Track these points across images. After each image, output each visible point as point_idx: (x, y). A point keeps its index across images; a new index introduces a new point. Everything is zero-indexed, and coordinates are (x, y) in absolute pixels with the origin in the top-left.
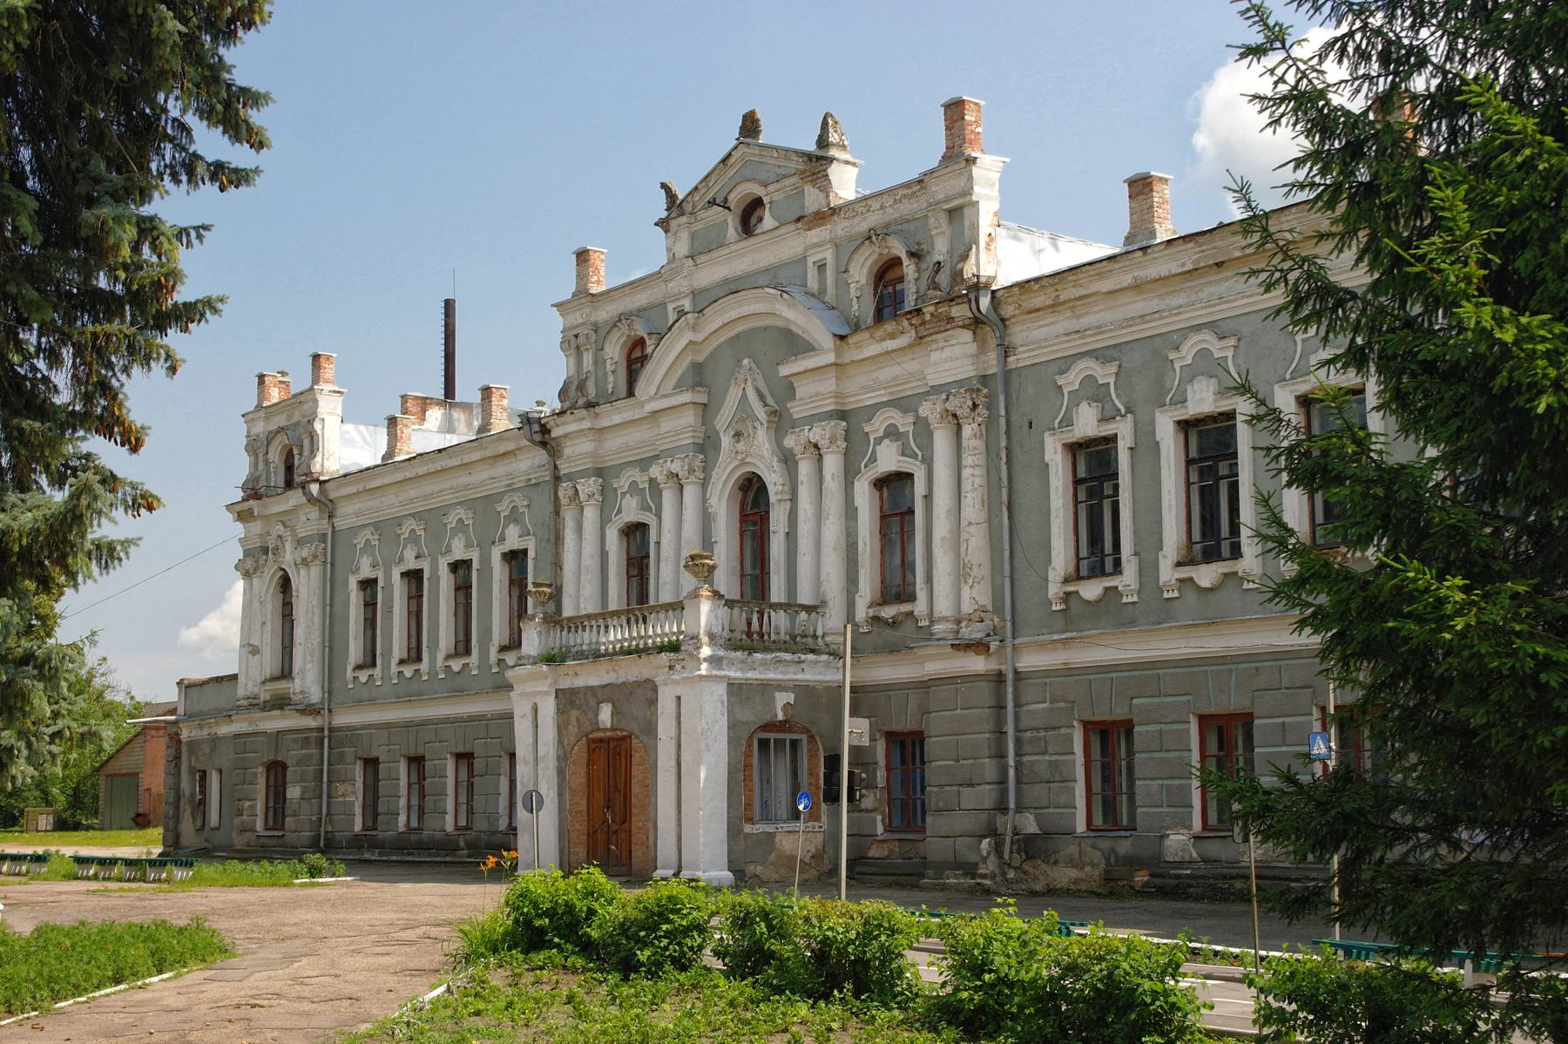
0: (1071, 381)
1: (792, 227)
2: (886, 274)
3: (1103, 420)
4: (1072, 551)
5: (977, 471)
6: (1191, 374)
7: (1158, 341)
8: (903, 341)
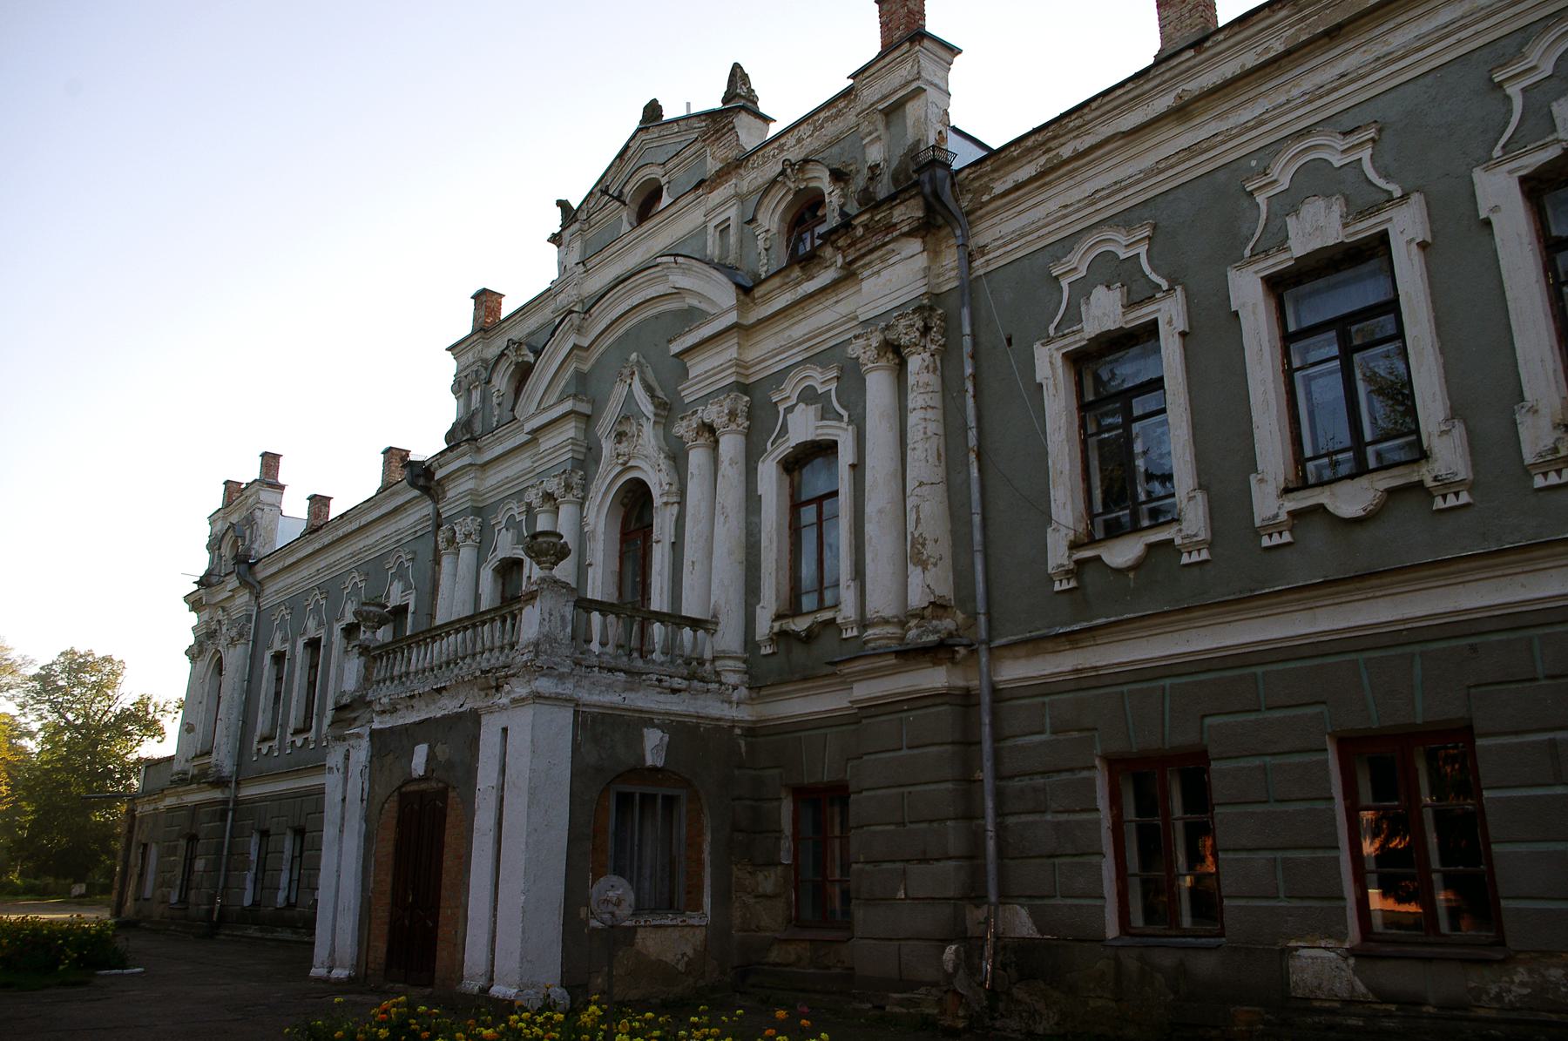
0: (1078, 262)
3: (1131, 305)
4: (1081, 506)
5: (930, 414)
6: (1290, 203)
7: (1221, 177)
8: (825, 277)
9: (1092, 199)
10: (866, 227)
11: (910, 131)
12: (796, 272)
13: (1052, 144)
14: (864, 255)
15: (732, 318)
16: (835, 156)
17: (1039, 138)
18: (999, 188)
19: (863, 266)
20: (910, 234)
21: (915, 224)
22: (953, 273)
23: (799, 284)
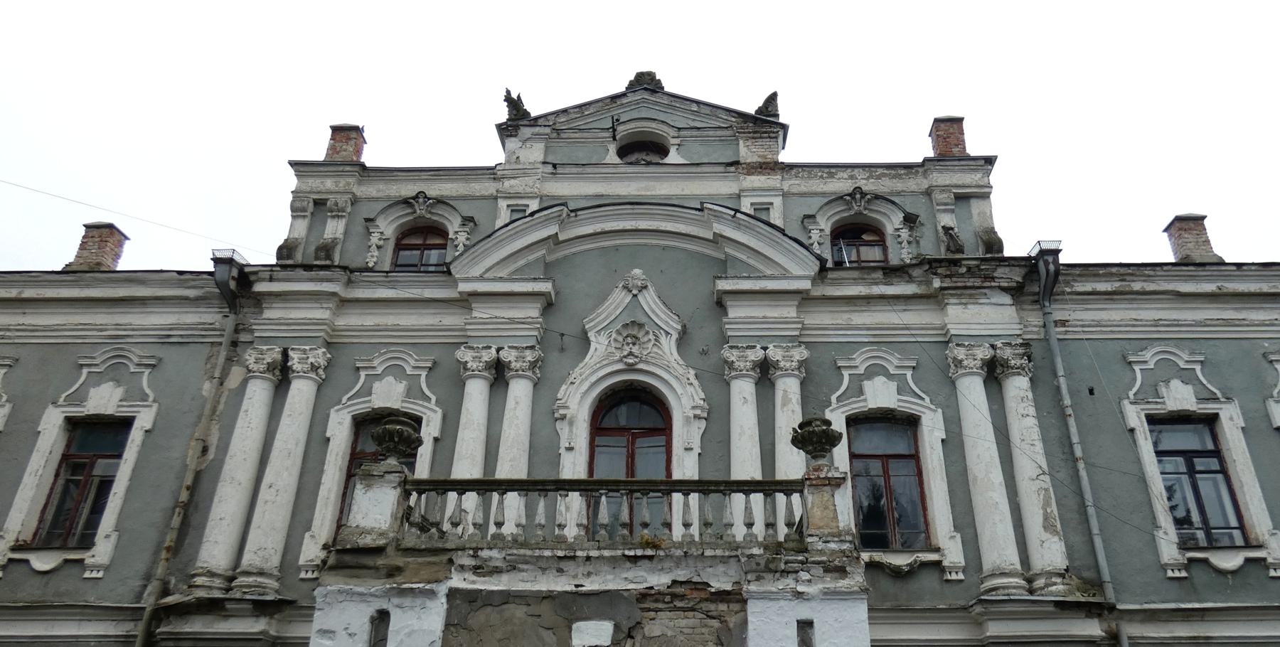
1: (721, 169)
2: (852, 231)
8: (909, 289)
9: (1156, 323)
10: (969, 269)
12: (879, 275)
13: (1128, 278)
15: (805, 285)
16: (917, 206)
17: (1122, 270)
18: (1080, 287)
23: (876, 284)
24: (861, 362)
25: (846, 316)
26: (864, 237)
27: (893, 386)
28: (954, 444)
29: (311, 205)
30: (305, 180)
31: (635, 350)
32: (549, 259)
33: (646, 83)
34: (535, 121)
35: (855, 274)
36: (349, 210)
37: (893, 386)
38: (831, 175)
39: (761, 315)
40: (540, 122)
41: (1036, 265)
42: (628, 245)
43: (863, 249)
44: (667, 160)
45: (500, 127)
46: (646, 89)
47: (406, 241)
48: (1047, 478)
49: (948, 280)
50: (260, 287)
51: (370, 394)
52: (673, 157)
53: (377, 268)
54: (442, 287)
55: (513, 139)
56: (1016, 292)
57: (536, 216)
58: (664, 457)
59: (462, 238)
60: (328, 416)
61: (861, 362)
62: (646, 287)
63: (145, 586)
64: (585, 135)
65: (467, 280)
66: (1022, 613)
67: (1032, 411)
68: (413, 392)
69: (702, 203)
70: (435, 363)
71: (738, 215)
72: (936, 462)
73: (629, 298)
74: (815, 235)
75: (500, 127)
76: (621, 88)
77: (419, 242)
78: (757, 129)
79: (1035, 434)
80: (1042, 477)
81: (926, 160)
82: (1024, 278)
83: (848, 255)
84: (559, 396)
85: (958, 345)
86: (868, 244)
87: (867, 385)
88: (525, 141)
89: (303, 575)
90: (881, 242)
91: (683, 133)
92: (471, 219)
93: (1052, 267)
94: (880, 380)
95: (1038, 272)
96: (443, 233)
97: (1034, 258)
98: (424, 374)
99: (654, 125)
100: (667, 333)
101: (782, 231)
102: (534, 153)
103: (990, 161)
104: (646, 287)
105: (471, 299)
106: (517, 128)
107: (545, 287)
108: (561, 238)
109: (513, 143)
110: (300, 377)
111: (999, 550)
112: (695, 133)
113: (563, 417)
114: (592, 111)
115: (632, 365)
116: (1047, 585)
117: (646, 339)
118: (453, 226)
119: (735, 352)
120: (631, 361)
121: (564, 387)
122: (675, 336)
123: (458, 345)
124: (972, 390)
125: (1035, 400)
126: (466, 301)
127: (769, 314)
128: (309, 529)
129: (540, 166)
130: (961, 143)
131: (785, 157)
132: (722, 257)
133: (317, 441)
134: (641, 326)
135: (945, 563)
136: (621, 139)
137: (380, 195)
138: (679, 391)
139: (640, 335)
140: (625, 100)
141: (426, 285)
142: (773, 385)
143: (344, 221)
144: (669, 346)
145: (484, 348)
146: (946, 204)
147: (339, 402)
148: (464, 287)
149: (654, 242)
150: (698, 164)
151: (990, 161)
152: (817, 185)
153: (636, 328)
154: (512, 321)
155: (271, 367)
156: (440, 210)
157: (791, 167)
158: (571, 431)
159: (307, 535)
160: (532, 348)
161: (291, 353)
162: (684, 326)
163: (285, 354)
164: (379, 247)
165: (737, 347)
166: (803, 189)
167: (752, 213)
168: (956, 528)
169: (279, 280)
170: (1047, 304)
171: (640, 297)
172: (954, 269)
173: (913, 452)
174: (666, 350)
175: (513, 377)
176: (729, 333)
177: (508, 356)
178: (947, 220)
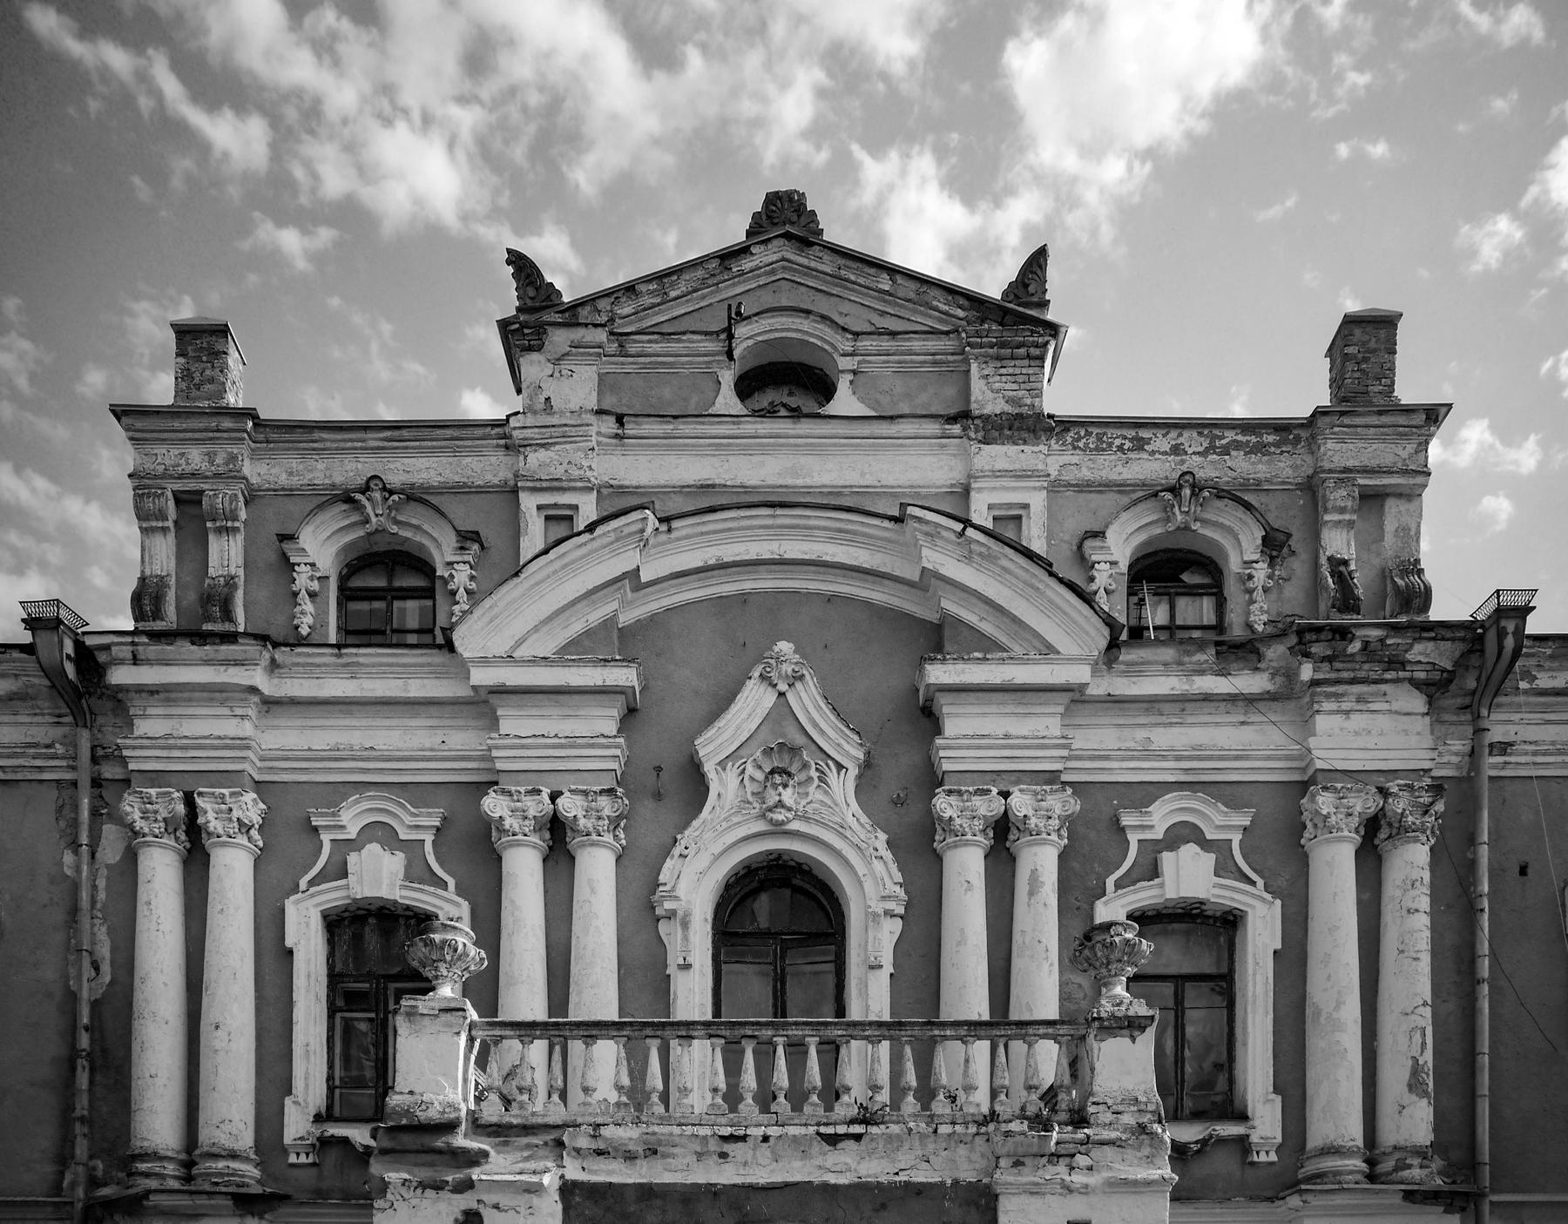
1: (932, 428)
11: (1389, 539)
12: (1207, 656)
14: (1338, 682)
19: (1329, 696)
20: (1416, 684)
21: (1436, 676)
22: (1455, 759)
23: (1201, 673)
24: (1161, 816)
25: (1141, 734)
26: (1186, 577)
27: (1209, 860)
28: (1293, 961)
29: (171, 503)
30: (148, 448)
31: (788, 796)
32: (625, 619)
33: (785, 217)
34: (572, 314)
35: (1168, 653)
36: (243, 515)
37: (1209, 860)
38: (1140, 444)
39: (1000, 732)
40: (584, 314)
41: (1481, 638)
42: (765, 593)
43: (1182, 602)
44: (834, 408)
45: (504, 325)
46: (788, 236)
47: (357, 582)
48: (1429, 1009)
49: (1326, 666)
50: (120, 676)
51: (345, 875)
52: (845, 401)
53: (316, 639)
54: (438, 676)
55: (535, 356)
56: (1434, 688)
57: (599, 531)
58: (831, 980)
59: (462, 577)
60: (283, 911)
61: (1161, 816)
62: (802, 678)
63: (62, 1173)
64: (674, 347)
65: (485, 661)
66: (1355, 1206)
67: (1424, 903)
68: (418, 873)
69: (903, 506)
70: (445, 818)
71: (970, 532)
72: (1260, 989)
73: (770, 698)
74: (1102, 576)
75: (504, 325)
76: (736, 233)
77: (381, 583)
78: (1008, 336)
79: (1422, 940)
80: (1421, 1010)
81: (1319, 413)
82: (1456, 664)
83: (1155, 614)
84: (662, 878)
85: (1325, 788)
86: (1193, 592)
87: (1167, 858)
88: (557, 361)
89: (293, 1159)
90: (1216, 589)
91: (866, 344)
92: (475, 536)
93: (1509, 642)
94: (1189, 850)
95: (1482, 651)
96: (424, 567)
97: (1482, 624)
98: (429, 838)
99: (805, 324)
100: (840, 767)
101: (1046, 565)
102: (577, 389)
103: (1433, 415)
104: (802, 678)
105: (494, 699)
106: (540, 330)
107: (625, 676)
108: (645, 577)
109: (534, 367)
110: (224, 844)
111: (1337, 1115)
112: (886, 344)
113: (671, 915)
114: (683, 287)
115: (782, 823)
116: (1396, 1169)
117: (802, 777)
118: (442, 549)
119: (953, 799)
120: (779, 816)
121: (669, 863)
122: (853, 771)
123: (483, 788)
124: (1335, 867)
125: (1432, 885)
126: (484, 705)
127: (1013, 732)
128: (289, 1092)
129: (591, 418)
130: (1387, 374)
131: (1058, 399)
132: (934, 617)
133: (274, 957)
134: (794, 751)
135: (1254, 1139)
136: (743, 357)
137: (295, 481)
138: (861, 869)
139: (793, 770)
140: (747, 264)
141: (406, 672)
142: (1013, 859)
143: (240, 537)
144: (843, 787)
145: (529, 792)
146: (1342, 510)
147: (295, 889)
148: (482, 677)
149: (813, 586)
150: (892, 418)
151: (1433, 415)
152: (1109, 467)
153: (786, 757)
154: (572, 741)
155: (170, 825)
156: (414, 514)
157: (1064, 426)
158: (686, 938)
159: (288, 1101)
160: (610, 792)
161: (199, 801)
162: (868, 754)
163: (189, 801)
164: (312, 595)
165: (960, 793)
166: (1086, 474)
167: (989, 525)
168: (1276, 1090)
169: (149, 662)
170: (1484, 712)
171: (790, 697)
172: (1340, 645)
173: (1224, 970)
174: (840, 799)
175: (582, 845)
176: (946, 766)
177: (570, 806)
178: (1337, 543)
